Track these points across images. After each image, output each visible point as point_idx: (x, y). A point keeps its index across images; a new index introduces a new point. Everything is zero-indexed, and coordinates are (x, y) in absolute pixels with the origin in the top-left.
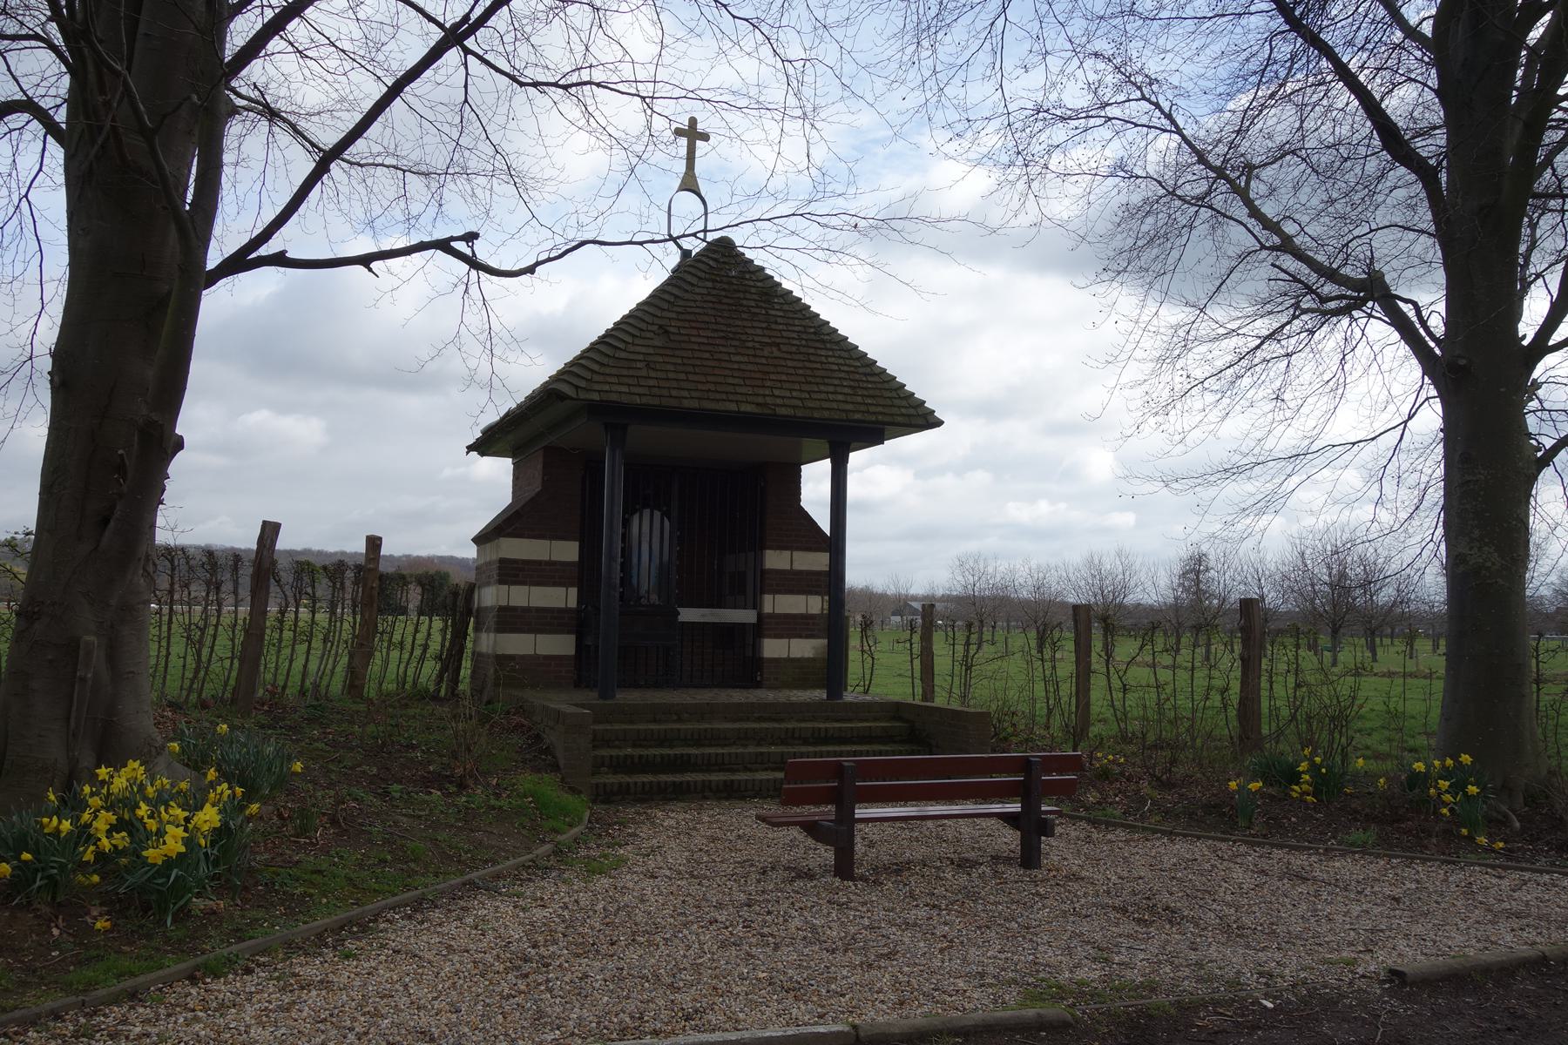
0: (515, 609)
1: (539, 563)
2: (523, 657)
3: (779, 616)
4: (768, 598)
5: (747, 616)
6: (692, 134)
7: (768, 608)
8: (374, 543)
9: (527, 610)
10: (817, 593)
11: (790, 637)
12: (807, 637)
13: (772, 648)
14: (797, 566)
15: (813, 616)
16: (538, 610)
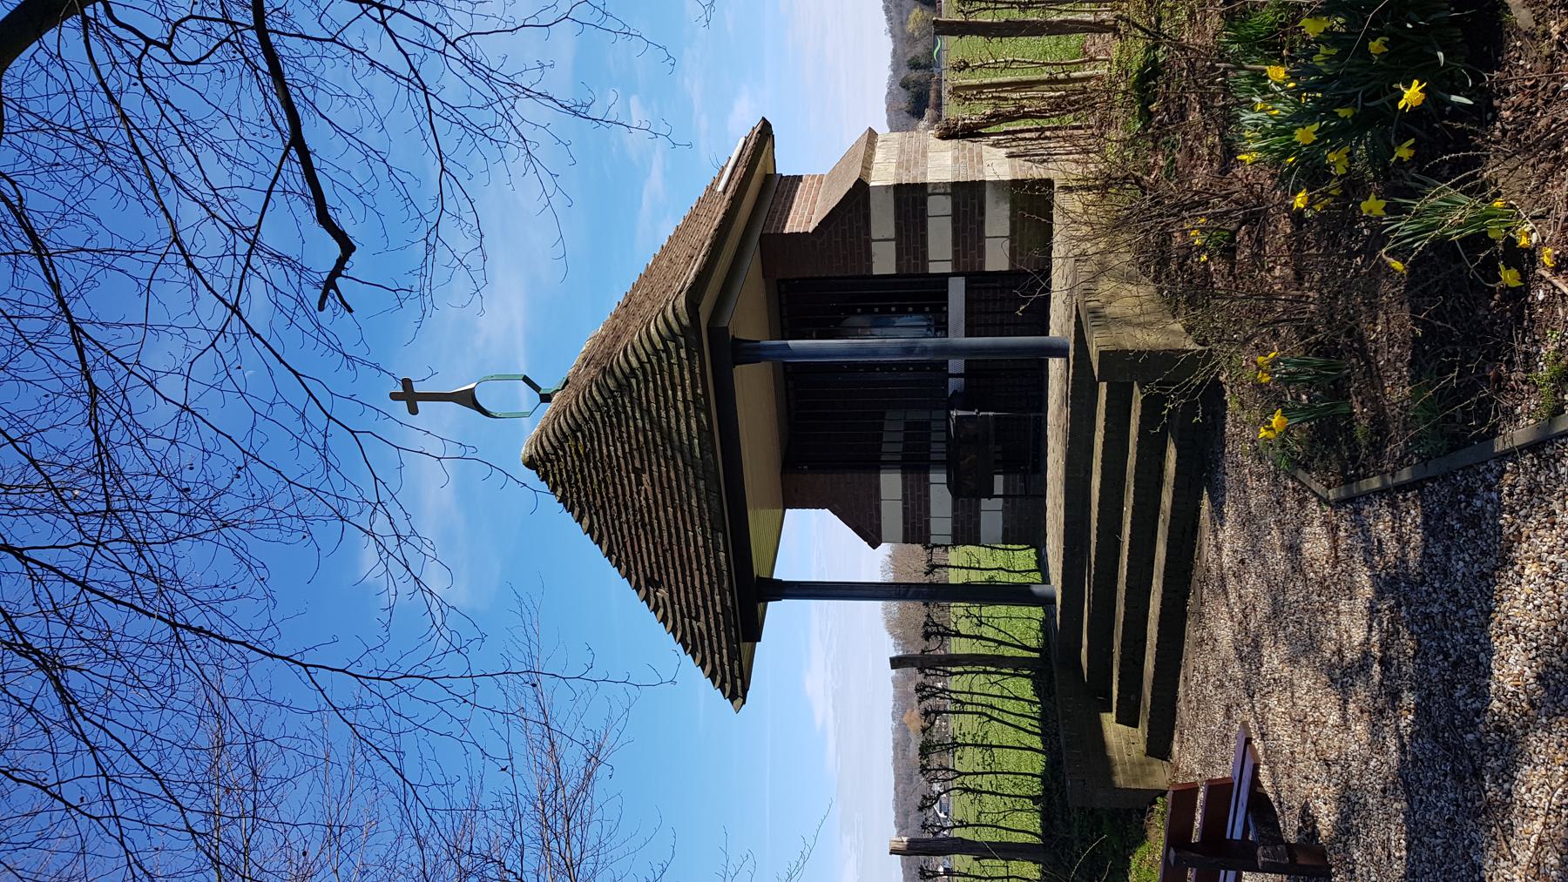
0: (954, 529)
1: (905, 510)
2: (1005, 521)
3: (955, 253)
4: (933, 269)
5: (957, 290)
6: (409, 396)
7: (947, 268)
8: (896, 663)
9: (955, 519)
10: (924, 203)
11: (981, 237)
12: (982, 213)
13: (997, 258)
14: (891, 232)
15: (955, 206)
16: (955, 509)
